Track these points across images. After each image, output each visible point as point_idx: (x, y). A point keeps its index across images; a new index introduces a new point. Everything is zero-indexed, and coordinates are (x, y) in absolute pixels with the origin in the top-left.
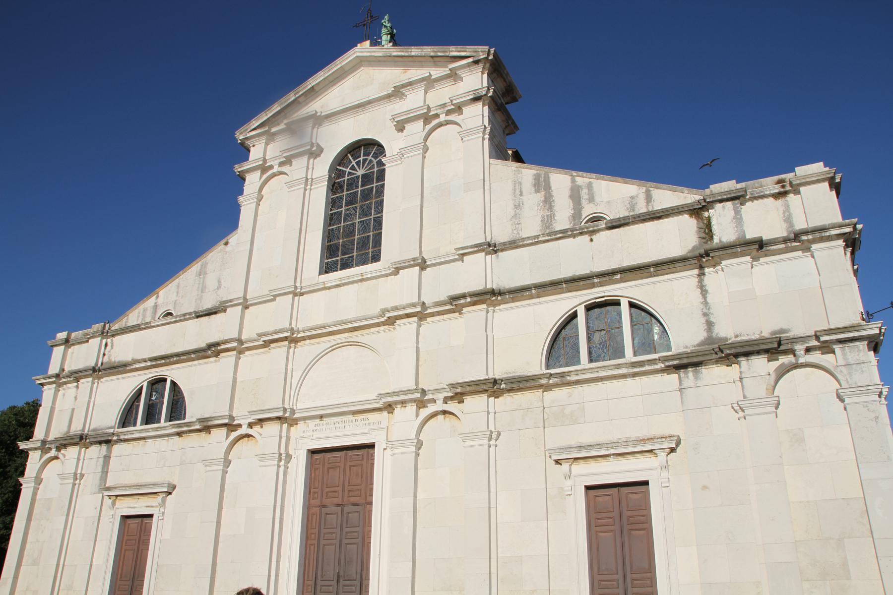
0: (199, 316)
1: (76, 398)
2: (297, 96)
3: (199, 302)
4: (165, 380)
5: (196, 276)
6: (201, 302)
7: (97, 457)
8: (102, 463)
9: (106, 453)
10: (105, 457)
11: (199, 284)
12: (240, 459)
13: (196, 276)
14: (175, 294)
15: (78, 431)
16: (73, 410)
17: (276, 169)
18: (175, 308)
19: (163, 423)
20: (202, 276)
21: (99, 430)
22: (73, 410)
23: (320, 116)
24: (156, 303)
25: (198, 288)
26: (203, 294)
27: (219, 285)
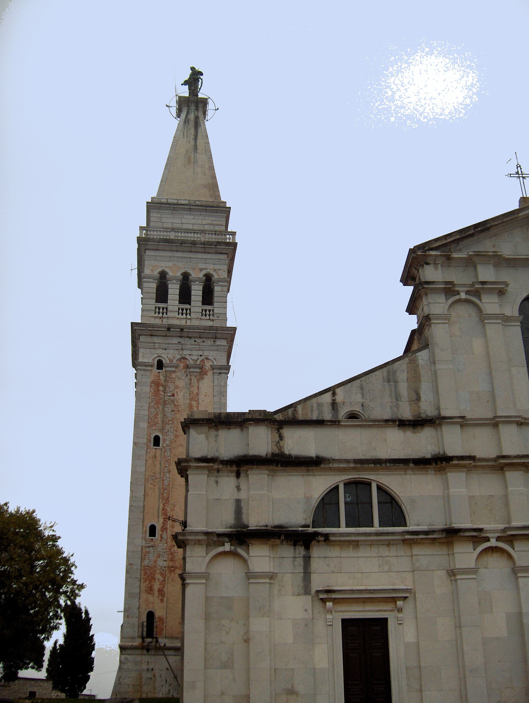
0: (402, 424)
1: (238, 488)
2: (476, 230)
3: (396, 410)
4: (369, 484)
5: (384, 382)
6: (398, 410)
7: (293, 556)
8: (302, 563)
9: (305, 553)
10: (304, 557)
11: (391, 391)
12: (488, 568)
13: (384, 382)
14: (359, 396)
15: (261, 526)
16: (238, 502)
17: (463, 296)
18: (363, 410)
19: (376, 528)
20: (392, 384)
21: (287, 528)
22: (238, 502)
23: (505, 257)
24: (334, 400)
25: (391, 394)
26: (399, 402)
27: (418, 396)
